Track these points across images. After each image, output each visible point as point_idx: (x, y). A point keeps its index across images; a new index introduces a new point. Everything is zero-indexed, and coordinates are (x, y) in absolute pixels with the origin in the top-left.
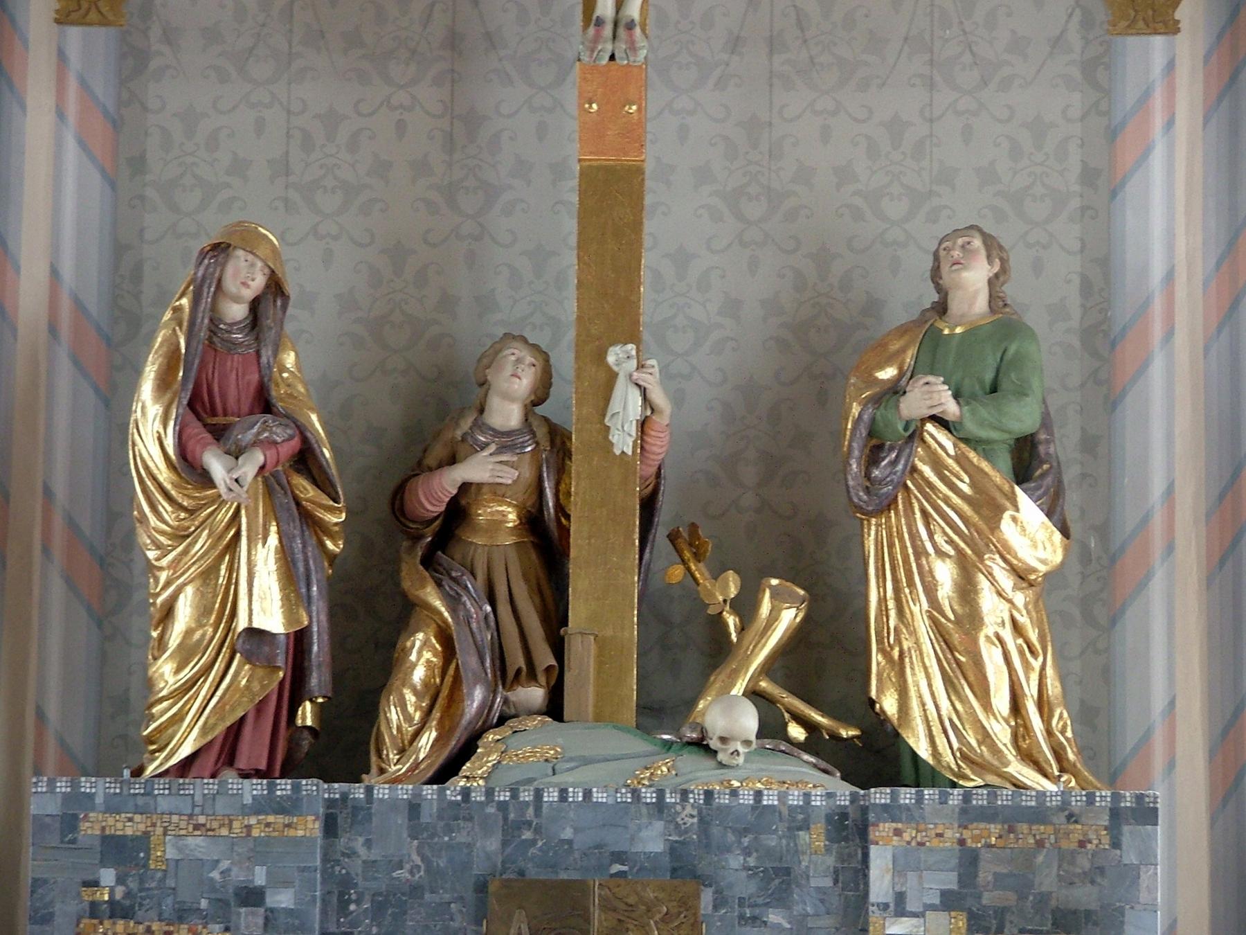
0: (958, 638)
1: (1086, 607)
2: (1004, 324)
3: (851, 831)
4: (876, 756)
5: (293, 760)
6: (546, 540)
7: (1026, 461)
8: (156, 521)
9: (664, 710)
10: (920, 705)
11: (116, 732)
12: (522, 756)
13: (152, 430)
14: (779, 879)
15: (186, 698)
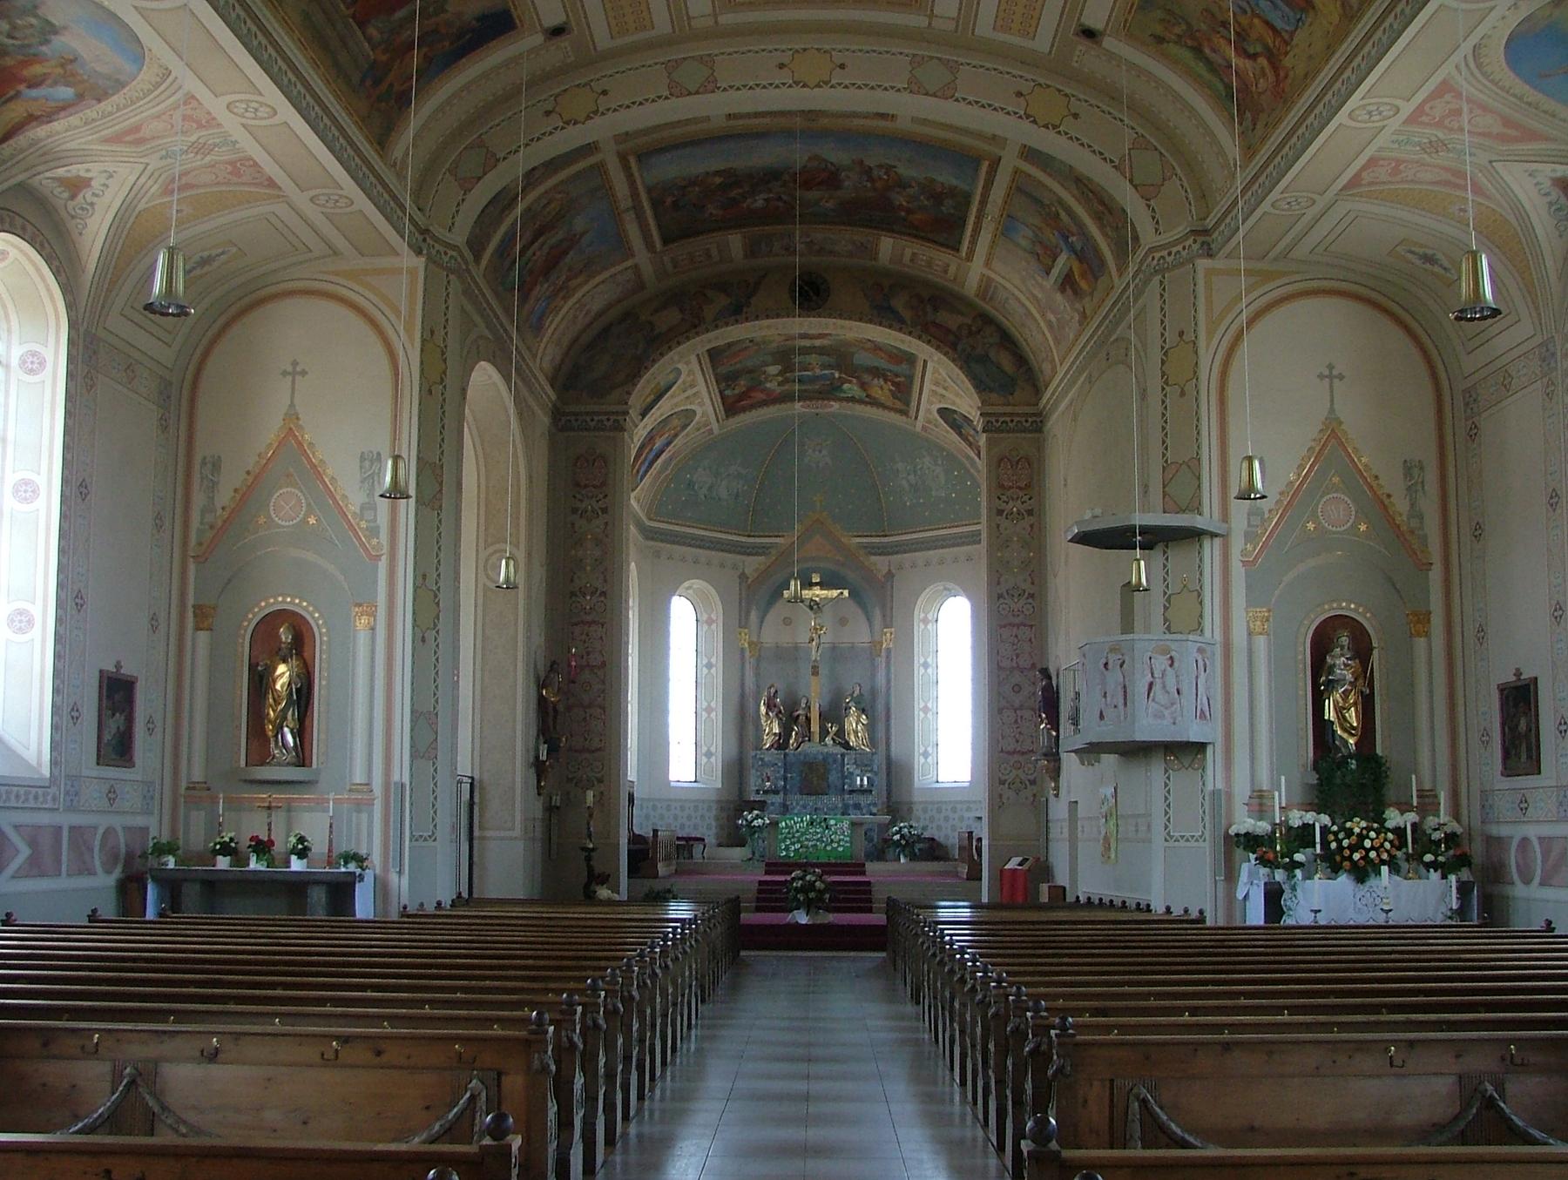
0: (856, 732)
1: (871, 728)
2: (861, 695)
3: (843, 755)
4: (846, 746)
5: (778, 748)
6: (808, 719)
7: (863, 711)
8: (763, 719)
9: (822, 739)
10: (853, 741)
11: (759, 747)
12: (805, 747)
13: (763, 709)
14: (835, 761)
15: (768, 741)
